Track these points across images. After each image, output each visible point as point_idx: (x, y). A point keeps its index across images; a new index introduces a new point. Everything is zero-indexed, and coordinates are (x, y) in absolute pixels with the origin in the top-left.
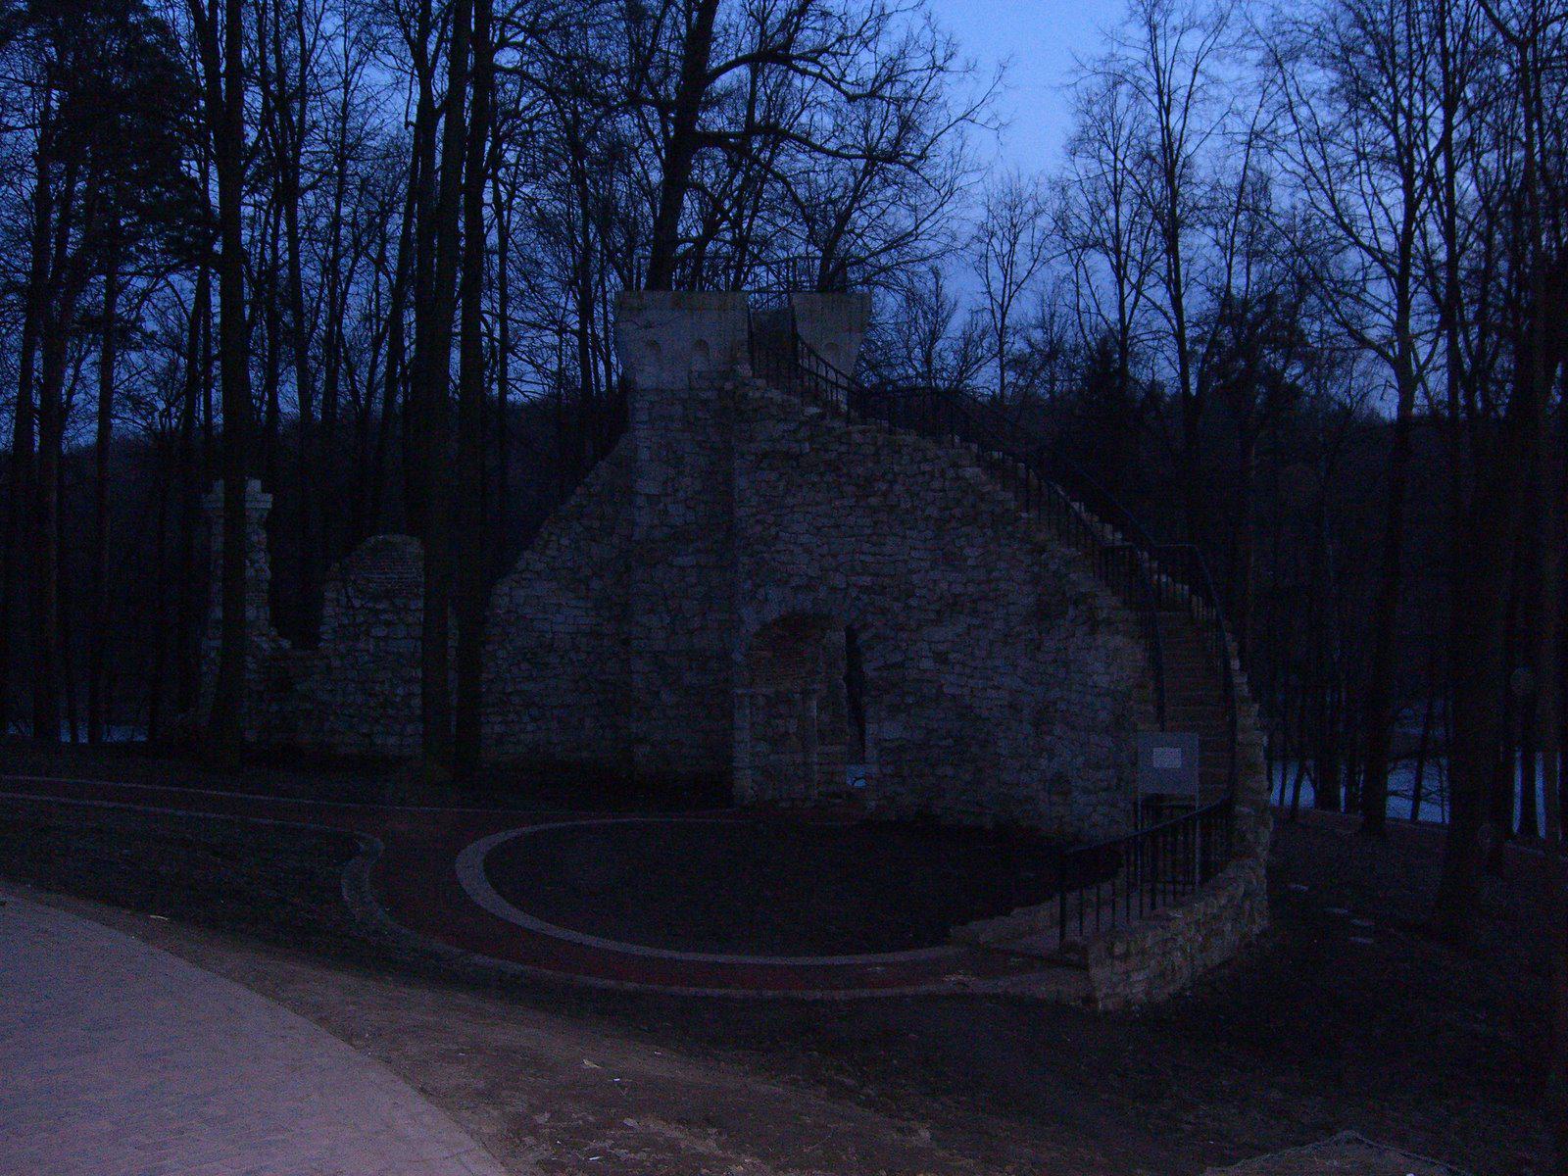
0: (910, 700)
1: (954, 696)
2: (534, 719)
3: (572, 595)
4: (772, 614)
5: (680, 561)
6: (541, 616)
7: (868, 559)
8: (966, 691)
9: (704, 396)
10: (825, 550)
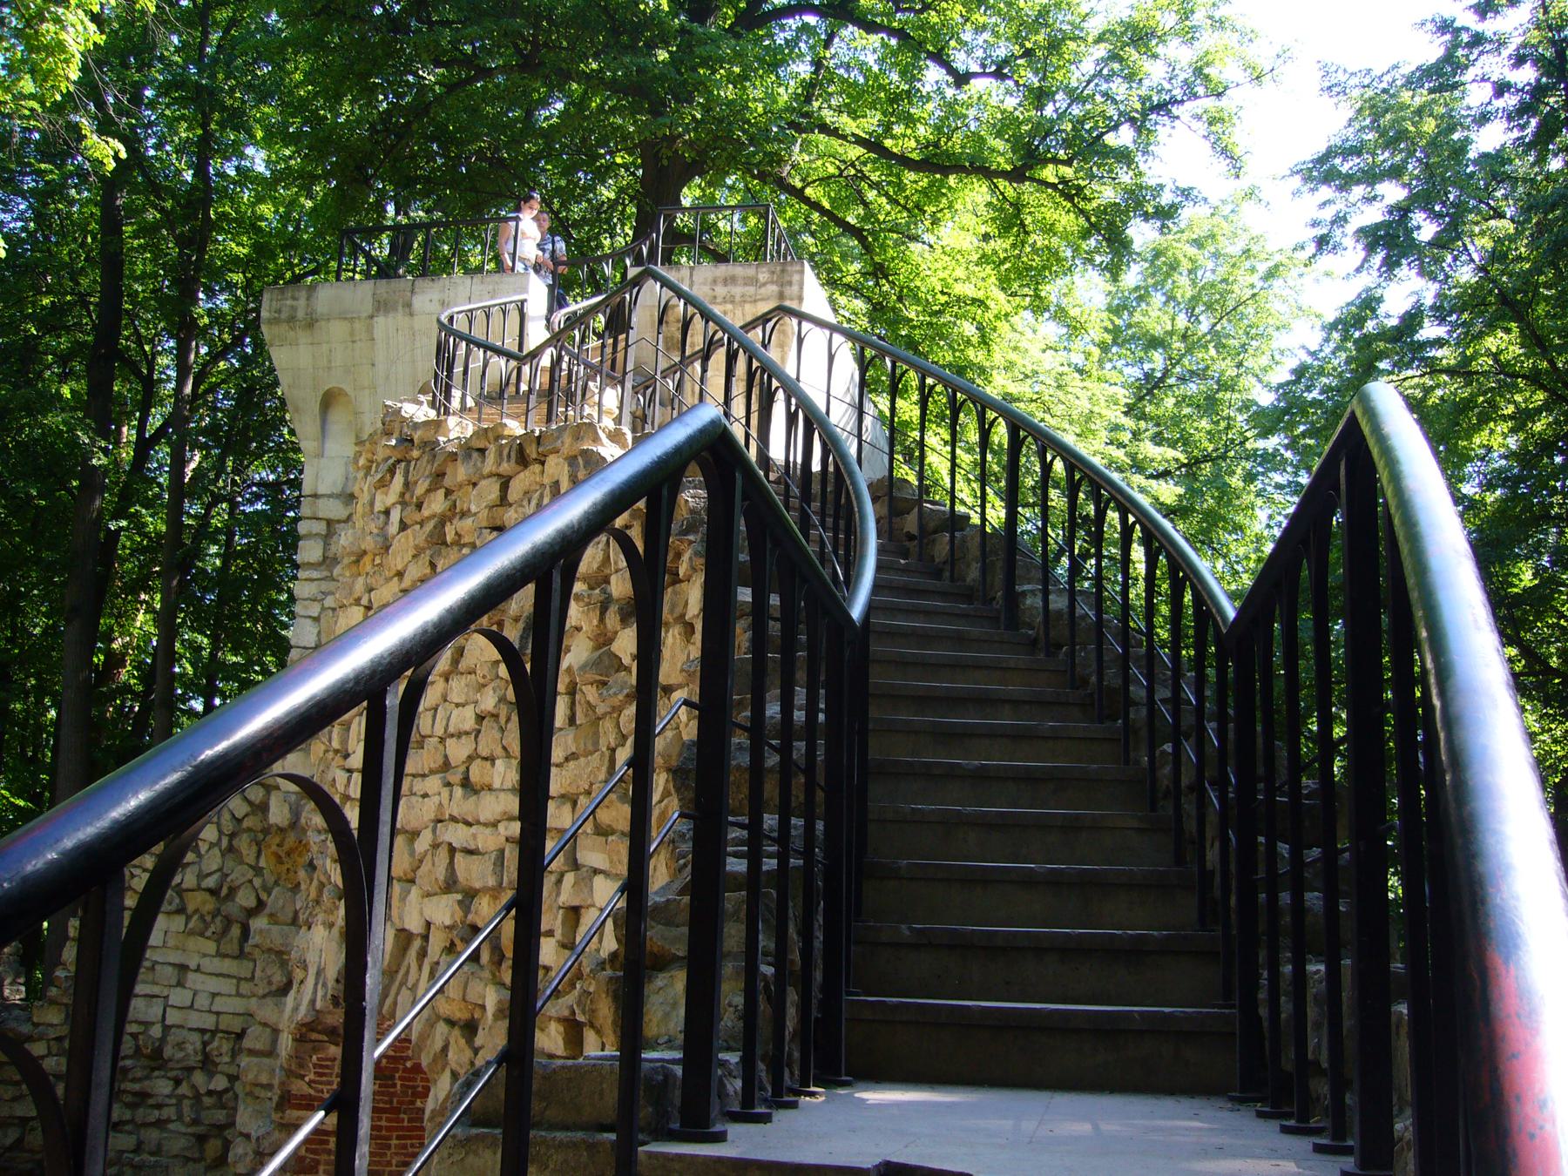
3: (211, 947)
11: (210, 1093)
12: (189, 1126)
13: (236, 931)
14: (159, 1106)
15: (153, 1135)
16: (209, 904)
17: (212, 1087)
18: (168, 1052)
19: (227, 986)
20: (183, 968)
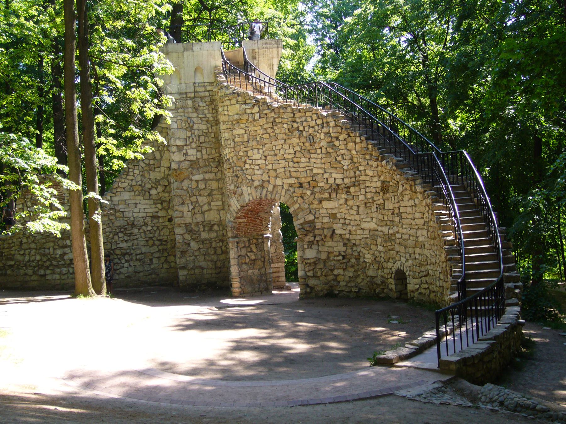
0: (318, 238)
1: (341, 235)
2: (127, 261)
3: (142, 198)
4: (247, 198)
5: (196, 177)
7: (293, 169)
8: (347, 232)
9: (202, 94)
10: (270, 167)
11: (147, 231)
13: (147, 194)
14: (136, 235)
15: (135, 242)
16: (140, 188)
18: (136, 223)
19: (148, 206)
20: (136, 204)
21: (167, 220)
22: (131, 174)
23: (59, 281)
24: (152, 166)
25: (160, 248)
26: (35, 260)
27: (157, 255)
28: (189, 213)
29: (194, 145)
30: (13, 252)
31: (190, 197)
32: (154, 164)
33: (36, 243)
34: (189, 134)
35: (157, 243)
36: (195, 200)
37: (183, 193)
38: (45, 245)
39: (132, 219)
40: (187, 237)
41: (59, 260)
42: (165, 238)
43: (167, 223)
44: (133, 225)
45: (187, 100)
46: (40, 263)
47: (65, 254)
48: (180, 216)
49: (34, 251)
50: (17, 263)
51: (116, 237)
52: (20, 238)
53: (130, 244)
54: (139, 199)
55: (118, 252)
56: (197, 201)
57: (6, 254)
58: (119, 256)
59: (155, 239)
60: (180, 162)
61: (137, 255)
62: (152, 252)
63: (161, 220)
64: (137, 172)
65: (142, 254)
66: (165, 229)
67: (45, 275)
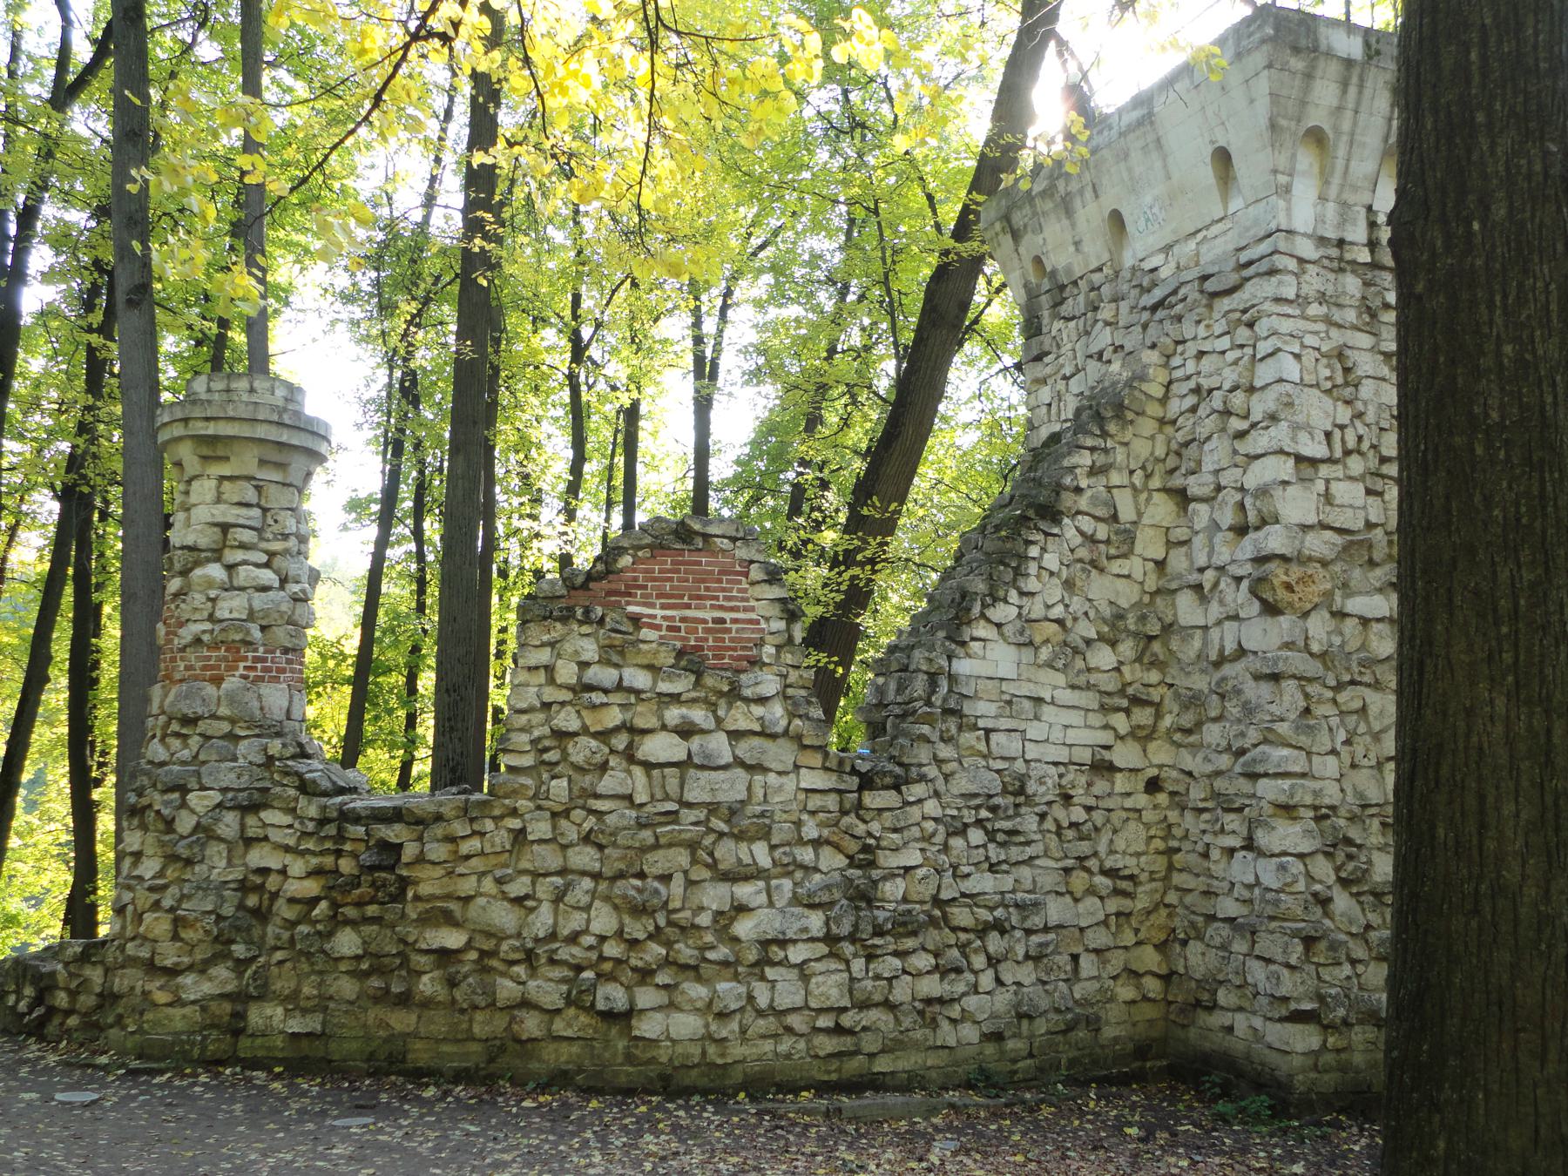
3: (1061, 679)
5: (1356, 605)
6: (1005, 723)
11: (1072, 825)
12: (1057, 860)
14: (1028, 843)
15: (1025, 873)
17: (1074, 819)
18: (1032, 787)
19: (1075, 718)
20: (1038, 700)
21: (1141, 786)
22: (1033, 568)
23: (695, 1050)
24: (1102, 547)
25: (1113, 905)
26: (586, 931)
27: (1099, 938)
28: (1331, 760)
29: (1356, 465)
30: (467, 886)
31: (1339, 687)
32: (1108, 542)
33: (601, 847)
34: (1344, 414)
35: (1100, 880)
36: (1357, 704)
37: (1313, 668)
38: (651, 857)
39: (1019, 766)
40: (1323, 869)
41: (709, 938)
42: (1129, 864)
43: (1142, 800)
44: (1018, 789)
45: (1342, 270)
46: (612, 949)
47: (741, 909)
48: (1297, 769)
49: (587, 883)
50: (487, 945)
51: (957, 843)
52: (514, 812)
53: (1007, 882)
54: (1051, 684)
55: (961, 916)
56: (1363, 710)
57: (425, 889)
58: (963, 936)
59: (1093, 864)
60: (1305, 528)
61: (1029, 932)
62: (1083, 924)
63: (1121, 783)
64: (1051, 561)
65: (1046, 929)
66: (1132, 825)
67: (623, 1018)
